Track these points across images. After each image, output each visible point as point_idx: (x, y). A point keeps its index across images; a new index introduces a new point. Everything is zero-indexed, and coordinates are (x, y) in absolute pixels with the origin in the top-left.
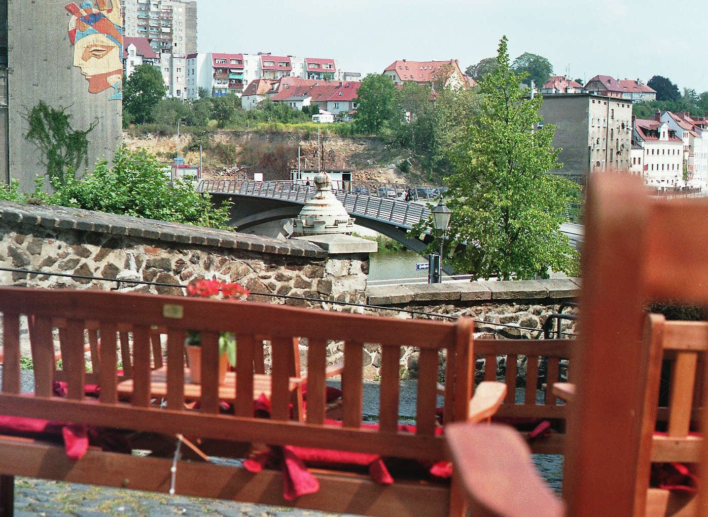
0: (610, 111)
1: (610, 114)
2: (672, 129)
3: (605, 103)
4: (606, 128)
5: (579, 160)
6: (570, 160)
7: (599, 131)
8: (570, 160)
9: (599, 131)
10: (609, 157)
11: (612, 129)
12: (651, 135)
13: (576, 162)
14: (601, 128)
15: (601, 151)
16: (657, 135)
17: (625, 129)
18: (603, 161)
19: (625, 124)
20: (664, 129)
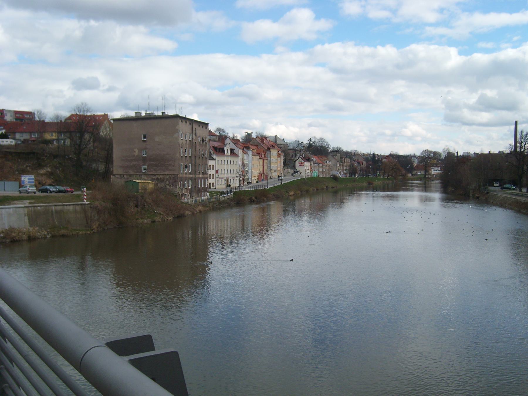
0: (194, 129)
1: (194, 132)
2: (232, 148)
3: (190, 124)
4: (191, 142)
5: (173, 164)
6: (167, 163)
7: (186, 143)
8: (167, 163)
9: (186, 143)
10: (193, 162)
11: (195, 142)
12: (219, 151)
13: (170, 165)
14: (188, 142)
15: (188, 158)
16: (223, 151)
17: (204, 143)
18: (190, 164)
19: (204, 139)
20: (227, 149)
